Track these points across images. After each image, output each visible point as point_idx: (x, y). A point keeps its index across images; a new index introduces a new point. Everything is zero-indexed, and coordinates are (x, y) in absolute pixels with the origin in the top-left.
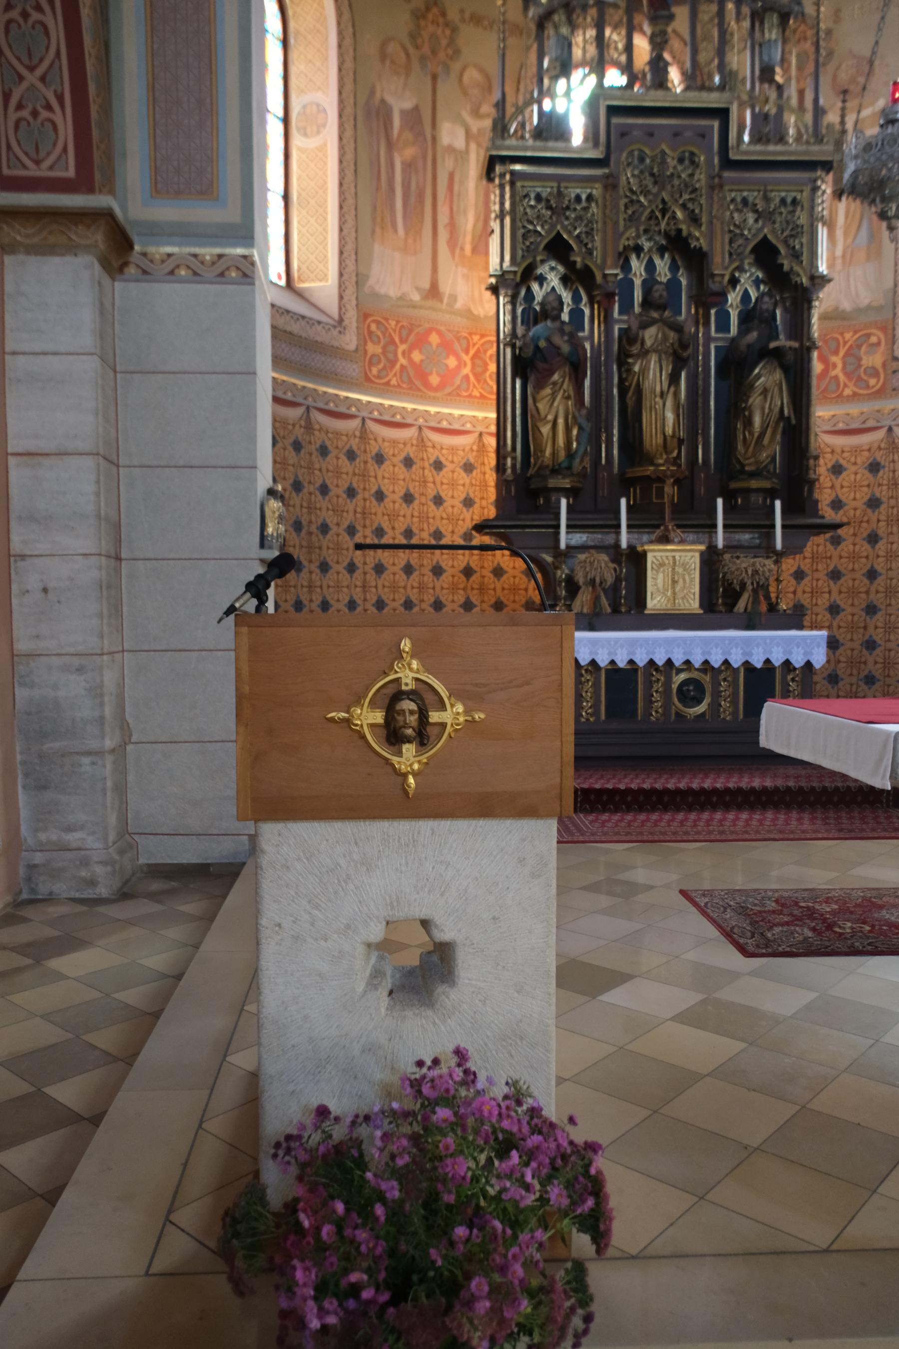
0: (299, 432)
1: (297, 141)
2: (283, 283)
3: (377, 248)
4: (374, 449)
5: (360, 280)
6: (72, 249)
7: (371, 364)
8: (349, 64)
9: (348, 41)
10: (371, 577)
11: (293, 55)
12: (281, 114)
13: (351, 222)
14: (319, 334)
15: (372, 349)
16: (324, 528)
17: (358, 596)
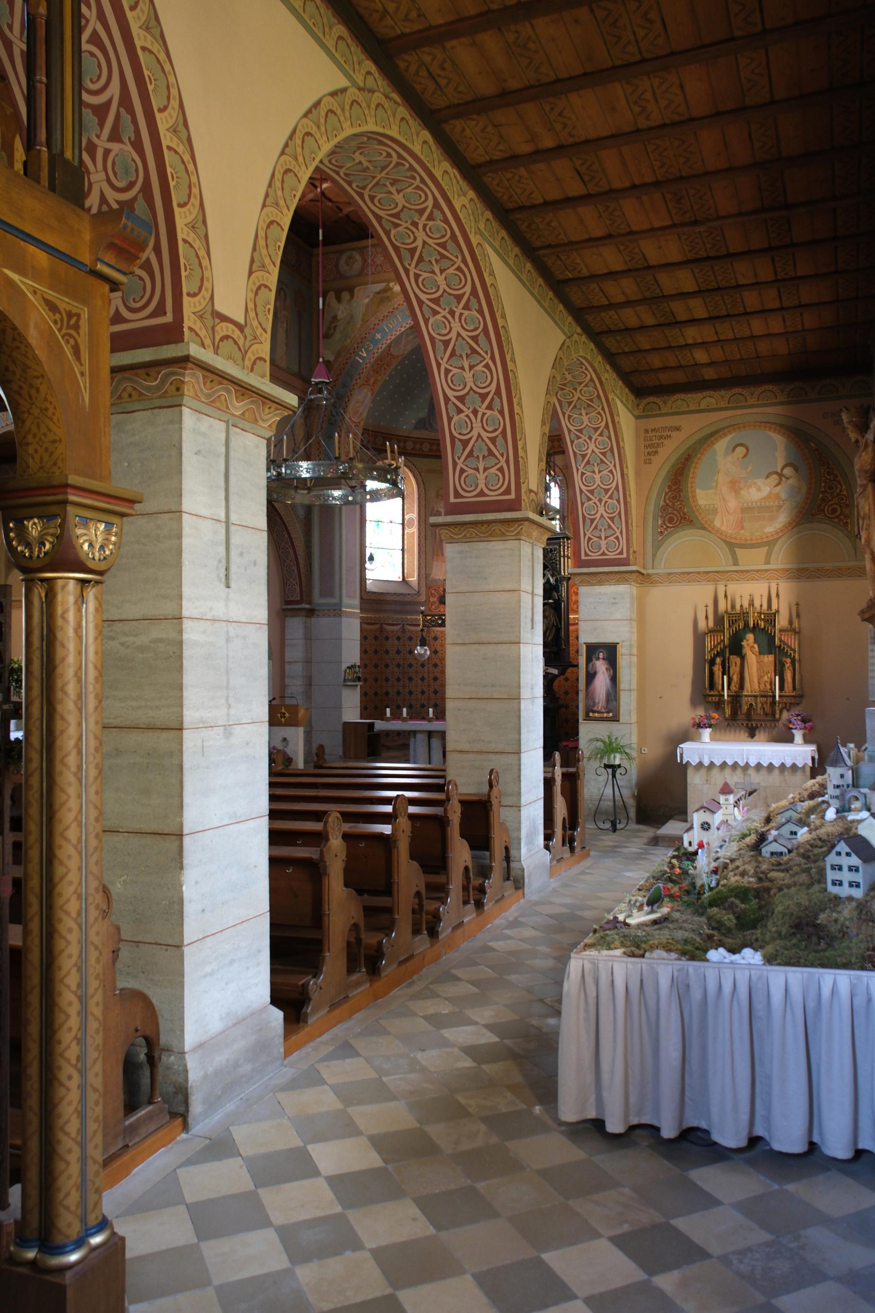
0: (399, 634)
1: (406, 531)
2: (401, 580)
3: (435, 563)
4: (433, 635)
5: (427, 576)
6: (298, 616)
7: (432, 605)
8: (423, 503)
9: (423, 495)
10: (432, 682)
11: (405, 501)
12: (401, 522)
13: (423, 557)
14: (410, 599)
15: (432, 599)
16: (411, 666)
17: (426, 689)
